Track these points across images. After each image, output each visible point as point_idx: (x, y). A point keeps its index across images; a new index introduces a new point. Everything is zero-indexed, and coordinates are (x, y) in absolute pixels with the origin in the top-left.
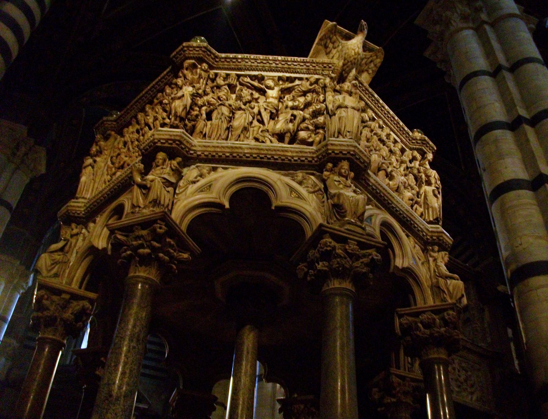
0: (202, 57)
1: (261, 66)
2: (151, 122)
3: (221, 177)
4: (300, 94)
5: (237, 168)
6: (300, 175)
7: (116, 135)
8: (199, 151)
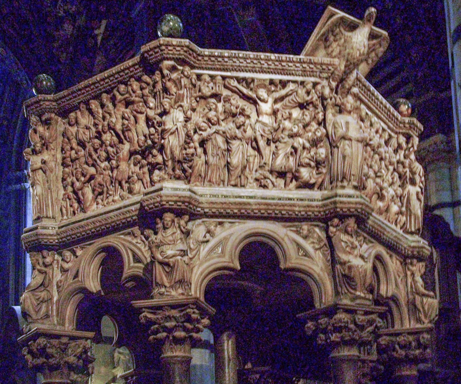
0: (183, 59)
1: (251, 67)
2: (119, 130)
3: (231, 235)
4: (295, 105)
5: (244, 223)
6: (305, 227)
7: (56, 117)
8: (207, 208)
